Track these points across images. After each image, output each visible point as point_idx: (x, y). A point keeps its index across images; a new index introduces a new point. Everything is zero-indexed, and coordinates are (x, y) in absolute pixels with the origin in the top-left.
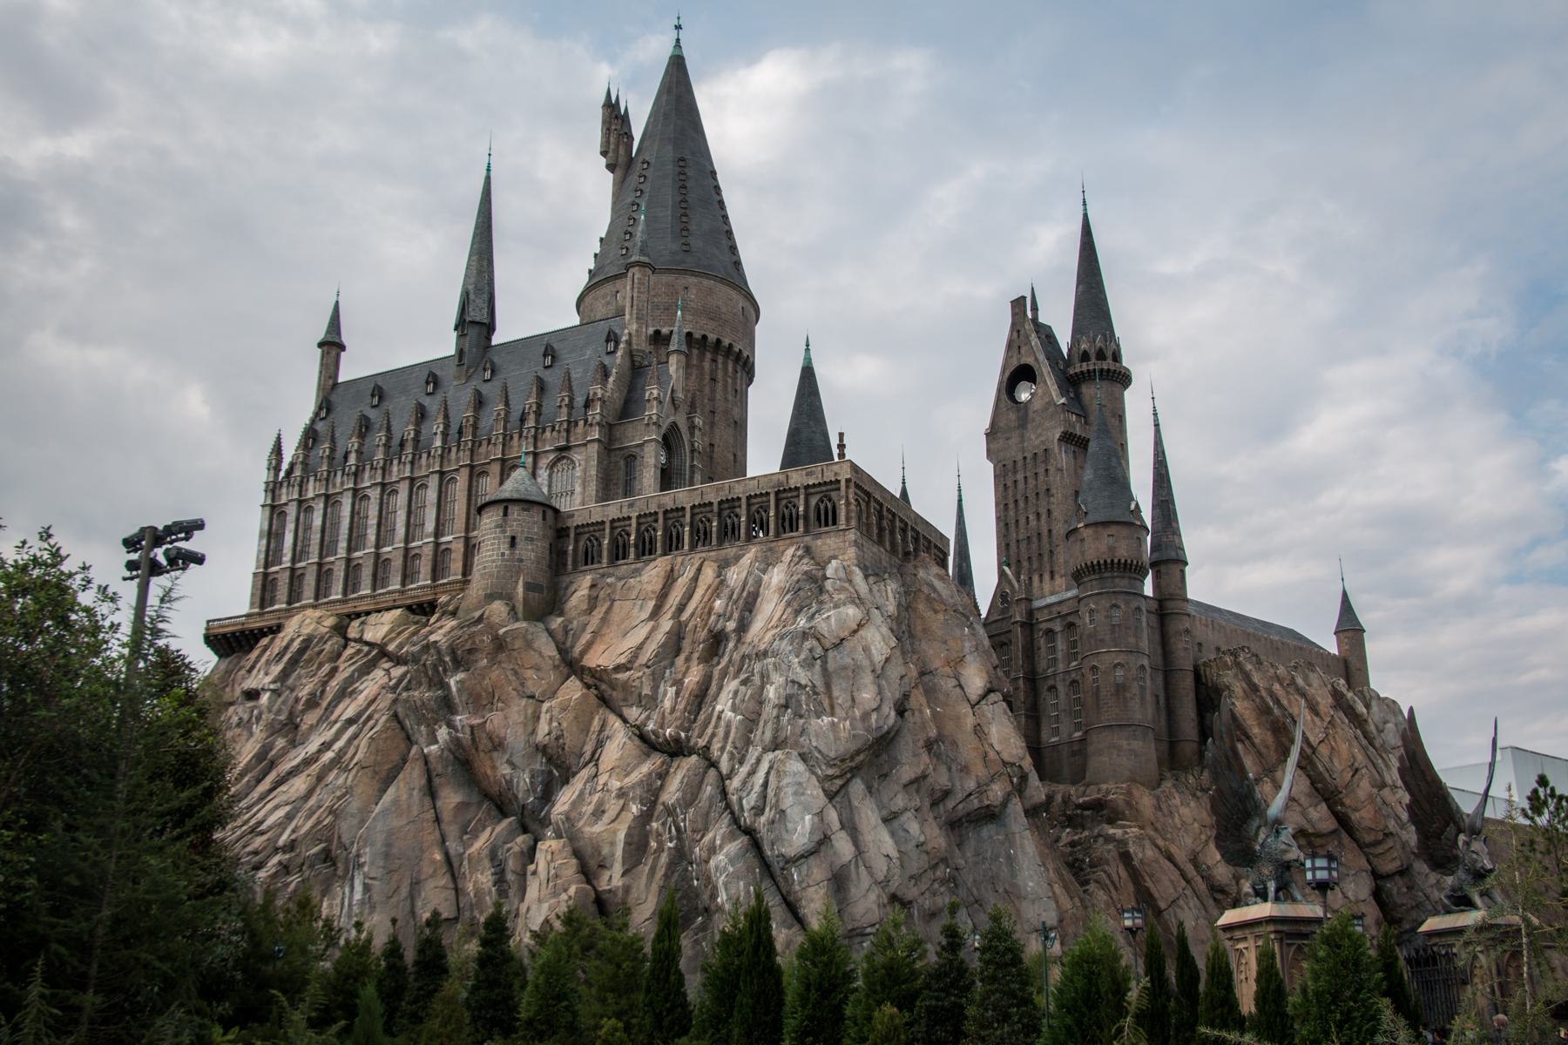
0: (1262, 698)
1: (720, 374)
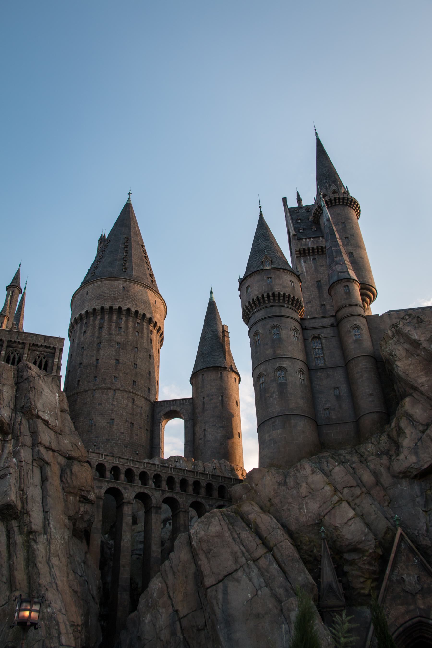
0: (424, 348)
1: (106, 323)
